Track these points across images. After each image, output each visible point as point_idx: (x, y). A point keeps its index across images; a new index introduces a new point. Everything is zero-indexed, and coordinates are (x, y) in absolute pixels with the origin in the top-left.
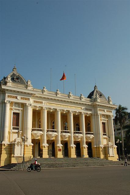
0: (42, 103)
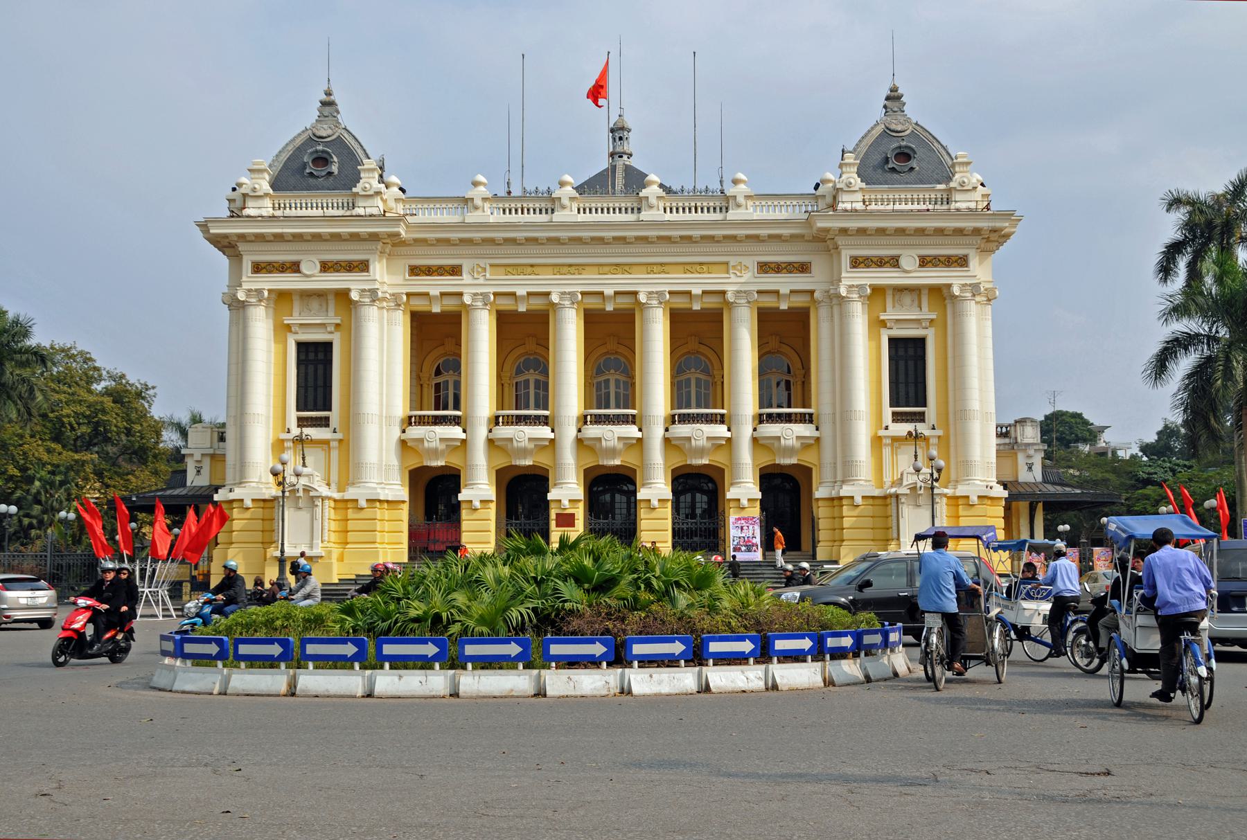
0: (455, 271)
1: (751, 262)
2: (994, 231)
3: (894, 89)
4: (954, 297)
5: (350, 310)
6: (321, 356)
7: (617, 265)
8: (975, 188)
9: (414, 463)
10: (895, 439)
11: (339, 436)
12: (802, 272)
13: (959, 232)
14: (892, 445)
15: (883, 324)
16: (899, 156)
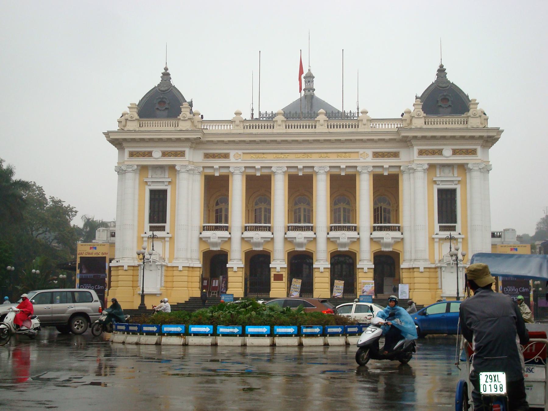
0: (226, 156)
1: (370, 152)
2: (489, 137)
3: (441, 66)
4: (470, 170)
5: (176, 175)
6: (161, 196)
7: (304, 153)
8: (480, 116)
9: (205, 248)
10: (440, 239)
11: (170, 235)
12: (395, 157)
13: (472, 138)
14: (439, 242)
15: (435, 182)
16: (444, 99)
